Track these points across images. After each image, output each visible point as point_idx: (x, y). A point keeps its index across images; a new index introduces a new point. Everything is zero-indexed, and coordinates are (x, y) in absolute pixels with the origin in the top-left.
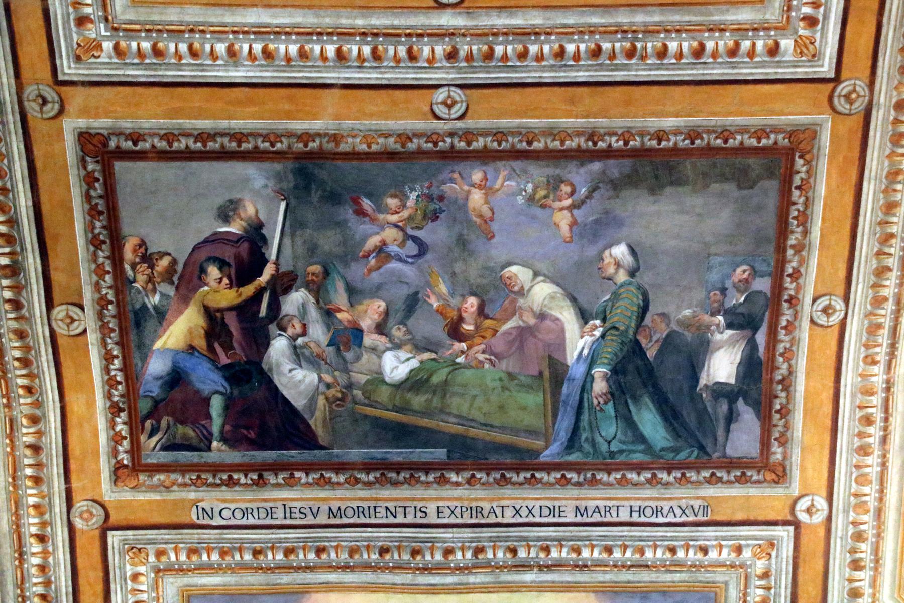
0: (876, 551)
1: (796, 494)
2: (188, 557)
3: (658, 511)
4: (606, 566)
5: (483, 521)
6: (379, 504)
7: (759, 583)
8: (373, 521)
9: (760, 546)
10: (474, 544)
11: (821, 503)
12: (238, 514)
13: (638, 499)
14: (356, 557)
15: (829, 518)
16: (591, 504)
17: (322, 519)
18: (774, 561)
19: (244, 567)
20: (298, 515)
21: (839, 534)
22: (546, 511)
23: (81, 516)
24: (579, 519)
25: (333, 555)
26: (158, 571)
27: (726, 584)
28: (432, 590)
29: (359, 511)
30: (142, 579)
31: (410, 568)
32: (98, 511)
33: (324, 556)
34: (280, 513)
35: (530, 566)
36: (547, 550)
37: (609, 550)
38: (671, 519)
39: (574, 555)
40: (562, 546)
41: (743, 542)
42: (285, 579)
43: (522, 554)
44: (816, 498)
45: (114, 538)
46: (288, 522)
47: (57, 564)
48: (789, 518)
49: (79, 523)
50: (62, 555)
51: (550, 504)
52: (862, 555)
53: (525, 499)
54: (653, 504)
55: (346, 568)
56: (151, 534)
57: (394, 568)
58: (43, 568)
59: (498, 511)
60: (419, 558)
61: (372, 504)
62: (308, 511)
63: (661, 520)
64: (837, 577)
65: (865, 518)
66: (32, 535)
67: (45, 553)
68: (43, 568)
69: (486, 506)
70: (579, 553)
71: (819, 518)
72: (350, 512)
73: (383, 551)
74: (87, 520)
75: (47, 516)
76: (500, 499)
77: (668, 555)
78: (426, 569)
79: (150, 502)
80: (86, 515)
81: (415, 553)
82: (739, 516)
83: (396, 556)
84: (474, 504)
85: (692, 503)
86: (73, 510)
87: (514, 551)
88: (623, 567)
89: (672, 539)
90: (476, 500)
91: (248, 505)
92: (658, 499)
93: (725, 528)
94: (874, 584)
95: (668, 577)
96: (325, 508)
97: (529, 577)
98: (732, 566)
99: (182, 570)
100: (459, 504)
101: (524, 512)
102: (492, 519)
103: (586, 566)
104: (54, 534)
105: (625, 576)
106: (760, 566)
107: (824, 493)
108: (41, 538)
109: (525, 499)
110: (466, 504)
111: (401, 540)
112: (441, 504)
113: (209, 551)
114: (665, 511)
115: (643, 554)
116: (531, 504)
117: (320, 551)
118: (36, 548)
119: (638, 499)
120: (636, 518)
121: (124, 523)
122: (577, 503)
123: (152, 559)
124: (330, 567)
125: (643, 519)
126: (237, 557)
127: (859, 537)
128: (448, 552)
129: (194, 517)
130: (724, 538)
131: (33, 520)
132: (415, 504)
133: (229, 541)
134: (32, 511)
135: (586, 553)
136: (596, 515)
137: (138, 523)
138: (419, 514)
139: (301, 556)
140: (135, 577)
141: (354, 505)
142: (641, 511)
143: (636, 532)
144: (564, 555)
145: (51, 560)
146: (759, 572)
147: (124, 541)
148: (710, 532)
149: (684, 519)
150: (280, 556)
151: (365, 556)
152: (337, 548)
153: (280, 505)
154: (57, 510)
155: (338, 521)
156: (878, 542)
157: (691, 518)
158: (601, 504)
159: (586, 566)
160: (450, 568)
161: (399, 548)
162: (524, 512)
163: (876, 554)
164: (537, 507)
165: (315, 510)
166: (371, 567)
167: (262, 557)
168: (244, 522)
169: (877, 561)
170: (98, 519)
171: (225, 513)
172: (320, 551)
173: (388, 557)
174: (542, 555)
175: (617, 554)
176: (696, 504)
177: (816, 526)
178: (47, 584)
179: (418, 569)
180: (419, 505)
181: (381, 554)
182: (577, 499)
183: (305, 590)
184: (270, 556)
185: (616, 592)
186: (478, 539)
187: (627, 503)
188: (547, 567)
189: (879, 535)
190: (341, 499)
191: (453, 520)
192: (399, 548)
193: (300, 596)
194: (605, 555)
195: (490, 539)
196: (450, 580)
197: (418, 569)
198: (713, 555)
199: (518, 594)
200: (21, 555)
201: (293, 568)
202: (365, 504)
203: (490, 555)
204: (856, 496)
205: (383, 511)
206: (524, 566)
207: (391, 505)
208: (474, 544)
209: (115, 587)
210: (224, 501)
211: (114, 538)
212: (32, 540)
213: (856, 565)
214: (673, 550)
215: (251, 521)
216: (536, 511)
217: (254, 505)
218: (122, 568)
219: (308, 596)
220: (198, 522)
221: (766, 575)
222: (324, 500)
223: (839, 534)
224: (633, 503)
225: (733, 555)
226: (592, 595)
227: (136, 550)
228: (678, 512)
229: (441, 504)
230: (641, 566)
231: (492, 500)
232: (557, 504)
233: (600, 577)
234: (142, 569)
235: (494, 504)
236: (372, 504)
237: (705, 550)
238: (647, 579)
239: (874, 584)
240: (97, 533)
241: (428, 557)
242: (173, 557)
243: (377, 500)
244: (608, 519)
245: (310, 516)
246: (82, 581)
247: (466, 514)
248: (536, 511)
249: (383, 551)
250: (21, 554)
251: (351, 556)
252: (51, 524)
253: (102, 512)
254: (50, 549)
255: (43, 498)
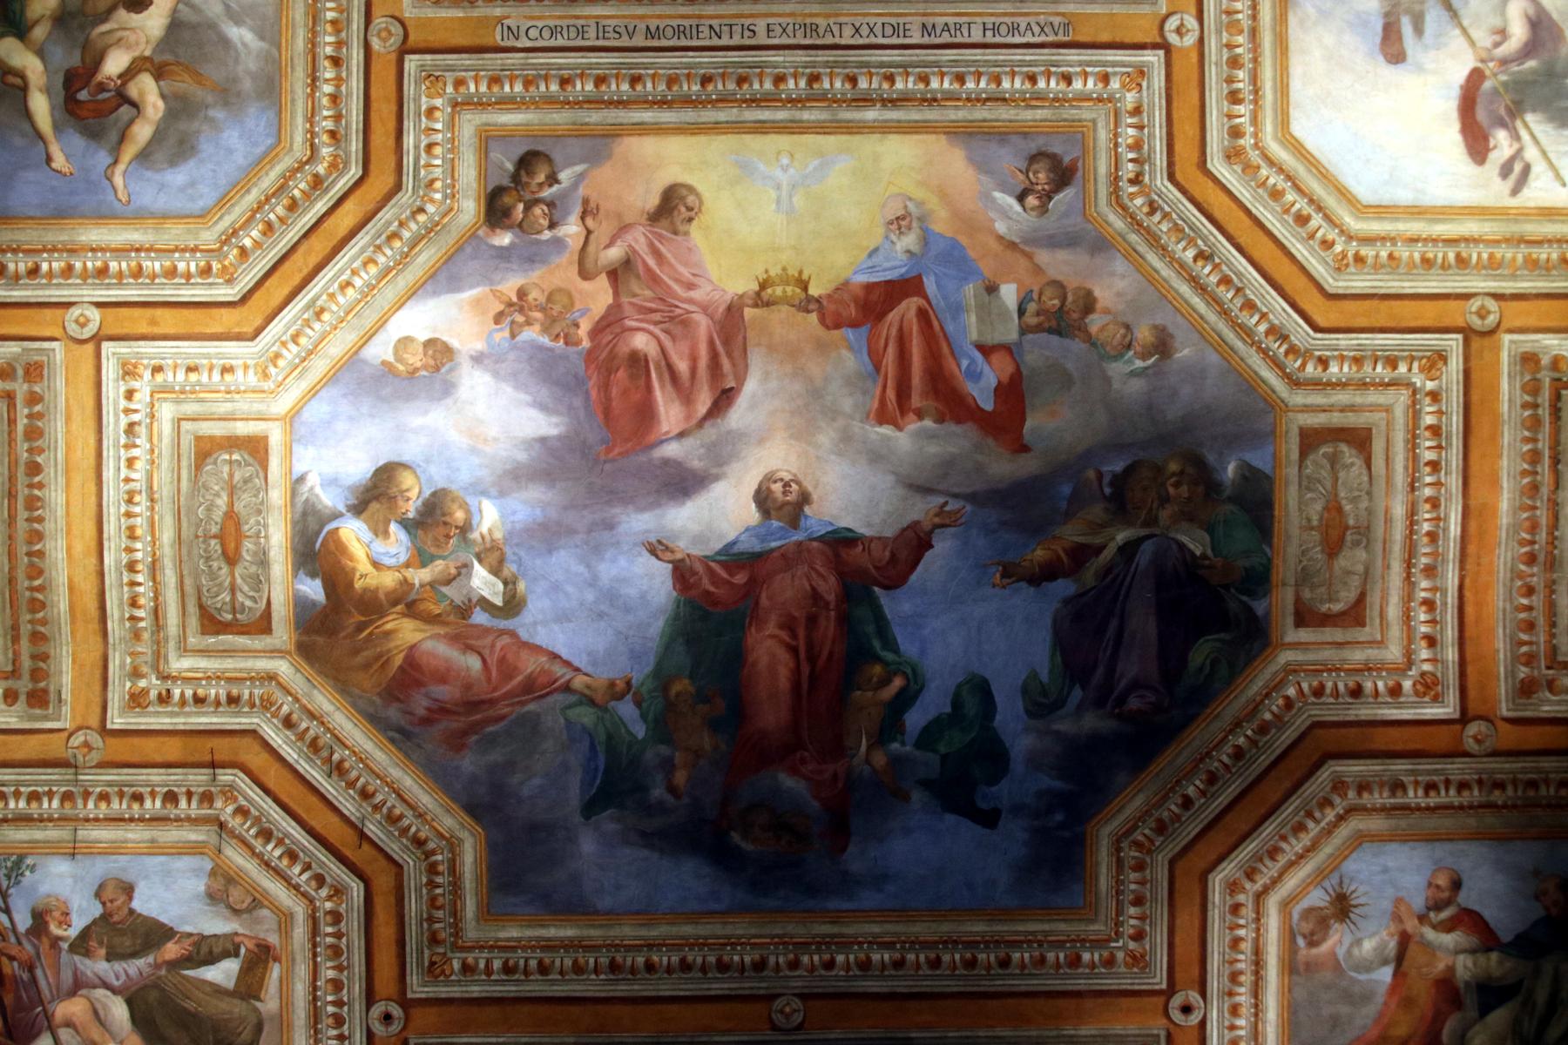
0: (1254, 78)
1: (1164, 11)
2: (489, 87)
3: (1013, 29)
4: (959, 99)
5: (819, 42)
6: (703, 21)
7: (1129, 121)
8: (695, 43)
9: (1128, 74)
10: (808, 71)
11: (1191, 22)
12: (546, 34)
13: (992, 15)
14: (675, 88)
15: (1201, 40)
16: (940, 21)
17: (639, 41)
18: (1145, 93)
19: (550, 101)
20: (612, 35)
21: (1214, 59)
22: (889, 30)
23: (378, 35)
24: (926, 40)
25: (649, 86)
26: (455, 105)
27: (1094, 121)
28: (761, 128)
29: (679, 31)
30: (438, 114)
31: (736, 101)
32: (396, 29)
33: (639, 88)
34: (592, 33)
35: (872, 100)
36: (891, 79)
37: (960, 79)
38: (1029, 39)
39: (921, 86)
40: (908, 74)
41: (1109, 70)
42: (594, 117)
43: (863, 84)
44: (1186, 17)
45: (412, 63)
46: (600, 43)
47: (349, 94)
48: (1158, 40)
49: (376, 44)
50: (355, 84)
51: (893, 21)
52: (1241, 85)
53: (865, 15)
54: (1008, 20)
55: (663, 103)
56: (451, 59)
57: (717, 101)
58: (334, 98)
59: (836, 29)
60: (746, 86)
61: (694, 22)
62: (622, 30)
63: (1017, 40)
64: (1215, 112)
65: (1240, 39)
66: (327, 57)
67: (338, 80)
68: (334, 98)
69: (822, 22)
70: (928, 84)
71: (1190, 40)
72: (669, 32)
73: (706, 80)
74: (384, 40)
75: (343, 34)
76: (837, 15)
77: (1028, 85)
78: (753, 101)
79: (452, 19)
80: (384, 34)
81: (741, 80)
82: (1105, 37)
83: (720, 87)
84: (808, 21)
85: (1051, 19)
86: (371, 27)
87: (853, 80)
88: (978, 100)
89: (1030, 64)
90: (811, 15)
91: (558, 22)
92: (1013, 15)
93: (1089, 51)
94: (1255, 120)
95: (1028, 115)
96: (642, 26)
97: (871, 114)
98: (1100, 100)
99: (480, 104)
100: (790, 20)
101: (865, 31)
102: (829, 40)
103: (935, 100)
104: (349, 57)
105: (981, 113)
106: (1130, 98)
107: (1193, 10)
108: (336, 61)
109: (865, 15)
110: (799, 20)
111: (726, 65)
112: (771, 21)
113: (512, 80)
114: (1022, 29)
115: (999, 83)
116: (872, 20)
117: (635, 80)
118: (329, 74)
119: (992, 15)
120: (989, 38)
121: (422, 45)
122: (924, 19)
123: (450, 89)
124: (646, 102)
125: (998, 40)
126: (543, 88)
127: (1234, 62)
128: (779, 79)
129: (499, 38)
130: (1089, 64)
131: (329, 39)
132: (743, 21)
133: (534, 67)
134: (329, 28)
135: (935, 84)
136: (946, 34)
137: (437, 45)
138: (747, 33)
139: (614, 87)
140: (431, 111)
141: (675, 23)
142: (995, 29)
143: (990, 55)
144: (910, 85)
145: (343, 88)
146: (1130, 107)
147: (422, 68)
148: (1073, 55)
149: (1042, 39)
150: (590, 87)
151: (685, 87)
152: (653, 77)
153: (592, 22)
154: (355, 27)
155: (655, 43)
156: (1255, 69)
157: (1051, 38)
158: (951, 20)
159: (935, 100)
160: (780, 100)
161: (723, 76)
162: (865, 31)
163: (1255, 84)
164: (879, 25)
165: (631, 29)
166: (692, 102)
167: (569, 88)
168: (552, 43)
169: (1256, 92)
170: (395, 41)
171: (533, 33)
172: (635, 80)
173: (710, 87)
174: (886, 86)
175: (970, 85)
176: (1056, 20)
177: (1188, 49)
178: (338, 118)
179: (745, 101)
180: (747, 22)
181: (703, 85)
182: (924, 15)
183: (614, 133)
184: (579, 87)
185: (970, 134)
186: (813, 65)
187: (979, 20)
188: (892, 101)
189: (1255, 60)
190: (659, 17)
191: (785, 41)
192: (723, 76)
193: (609, 140)
194: (956, 86)
195: (826, 64)
196: (781, 115)
197: (745, 101)
198: (1077, 85)
199: (858, 137)
200: (314, 81)
201: (603, 102)
202: (686, 23)
203: (827, 85)
204: (1229, 13)
205: (706, 30)
206: (865, 100)
207: (715, 23)
208: (808, 71)
209: (409, 125)
210: (532, 18)
211: (412, 63)
212: (327, 63)
213: (1234, 97)
214: (1033, 79)
215: (560, 42)
216: (878, 30)
217: (564, 23)
218: (417, 100)
219: (619, 140)
220: (502, 44)
221: (1137, 111)
222: (642, 17)
223: (1214, 59)
224: (986, 19)
225: (1100, 85)
226: (943, 137)
227: (432, 78)
228: (1037, 29)
229: (771, 21)
230: (997, 100)
231: (828, 16)
232: (901, 20)
233: (953, 115)
234: (438, 102)
235: (831, 21)
236: (694, 22)
237: (1068, 79)
238: (1004, 116)
239: (1255, 120)
240: (393, 57)
241: (756, 86)
242: (472, 88)
243: (700, 17)
244: (959, 39)
245: (625, 37)
246: (374, 116)
247: (800, 33)
248: (878, 30)
249: (706, 80)
250: (314, 80)
251: (669, 88)
252: (346, 44)
253: (400, 31)
254: (344, 75)
255: (341, 12)
